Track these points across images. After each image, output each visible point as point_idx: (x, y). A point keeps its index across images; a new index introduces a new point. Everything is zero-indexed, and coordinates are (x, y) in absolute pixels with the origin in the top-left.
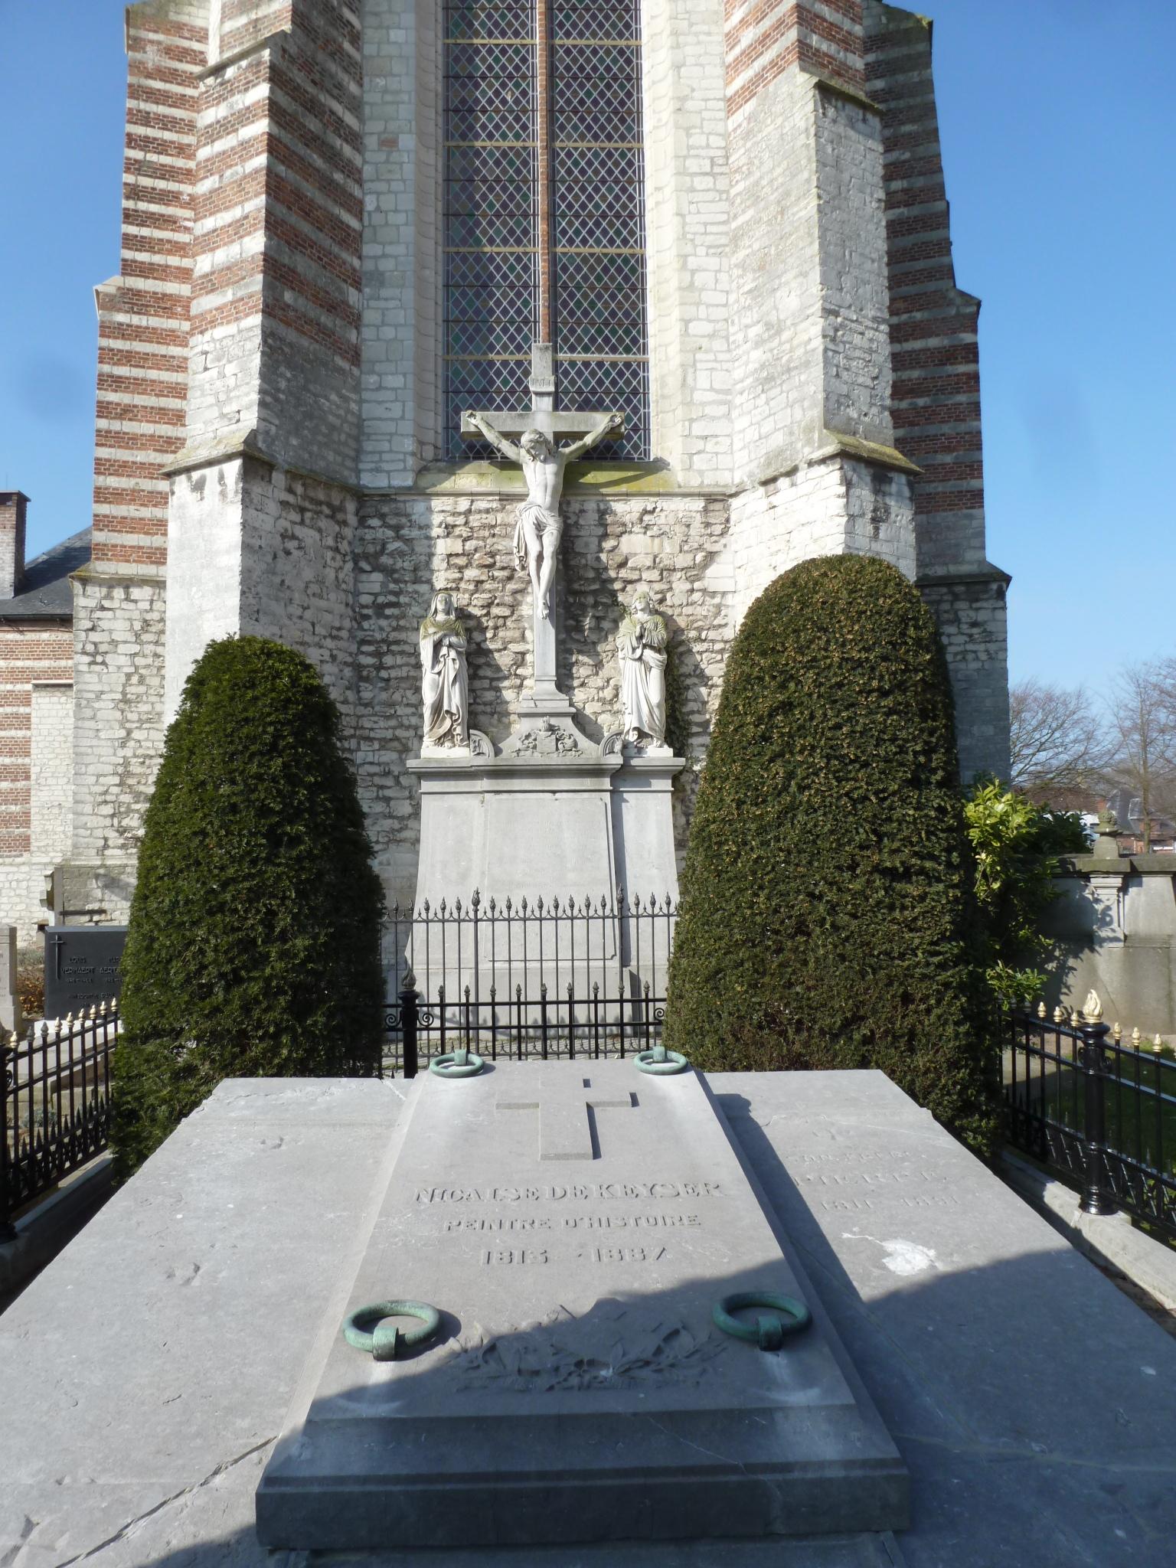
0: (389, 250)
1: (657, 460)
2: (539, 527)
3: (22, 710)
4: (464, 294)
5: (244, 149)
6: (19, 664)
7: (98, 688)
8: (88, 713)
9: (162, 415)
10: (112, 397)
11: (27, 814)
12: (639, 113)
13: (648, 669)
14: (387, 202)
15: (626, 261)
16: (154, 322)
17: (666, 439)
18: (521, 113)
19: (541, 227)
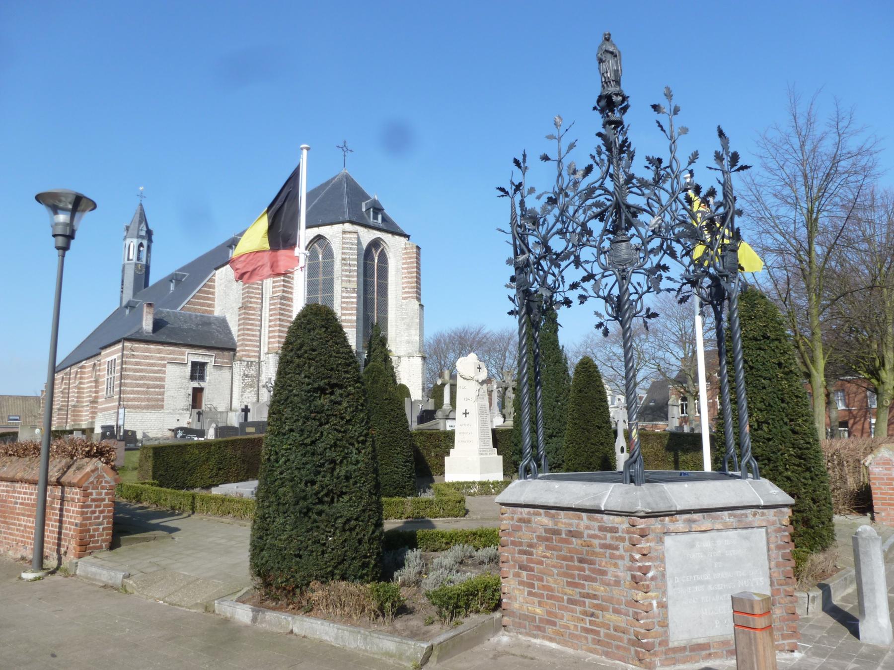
5: (352, 303)
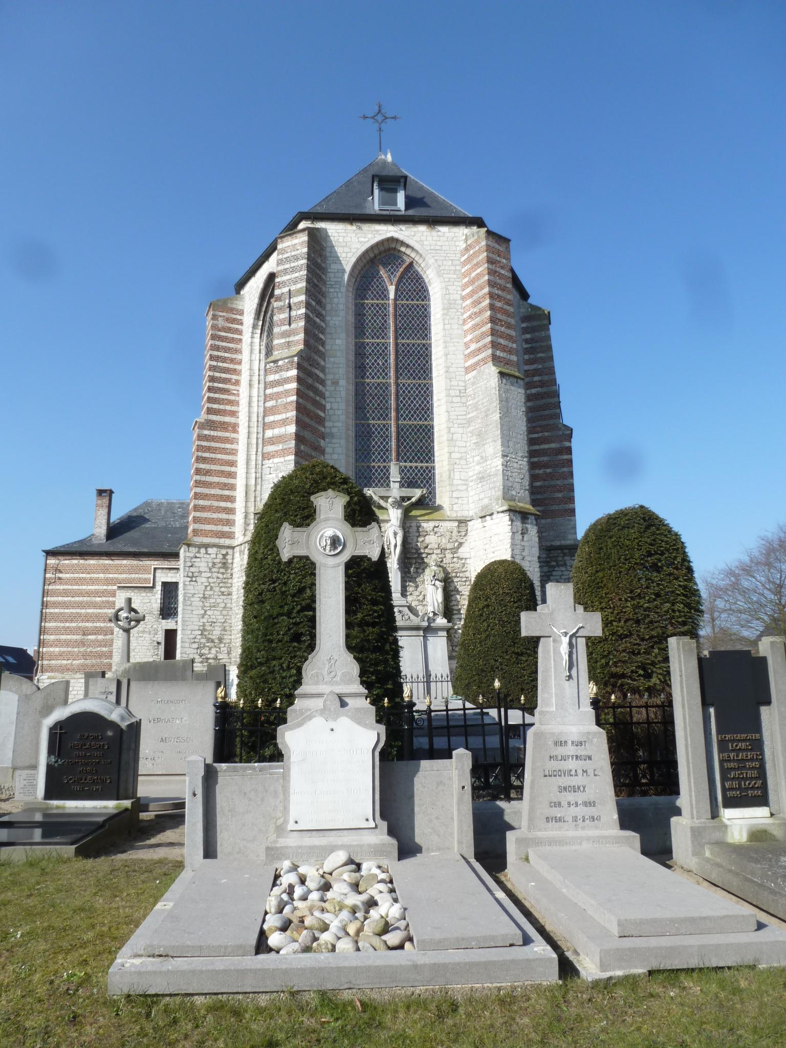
0: (336, 424)
1: (439, 506)
2: (395, 534)
3: (111, 599)
4: (363, 440)
5: (287, 393)
6: (111, 576)
7: (193, 592)
8: (189, 603)
9: (222, 473)
10: (202, 466)
11: (111, 652)
12: (431, 369)
13: (437, 588)
14: (335, 406)
15: (426, 427)
16: (219, 434)
17: (442, 498)
18: (386, 367)
19: (393, 414)
